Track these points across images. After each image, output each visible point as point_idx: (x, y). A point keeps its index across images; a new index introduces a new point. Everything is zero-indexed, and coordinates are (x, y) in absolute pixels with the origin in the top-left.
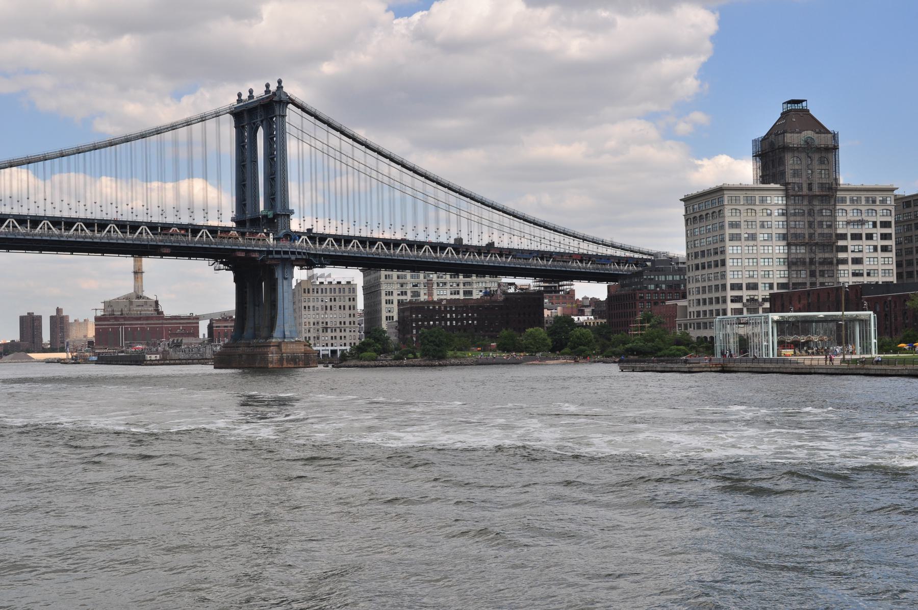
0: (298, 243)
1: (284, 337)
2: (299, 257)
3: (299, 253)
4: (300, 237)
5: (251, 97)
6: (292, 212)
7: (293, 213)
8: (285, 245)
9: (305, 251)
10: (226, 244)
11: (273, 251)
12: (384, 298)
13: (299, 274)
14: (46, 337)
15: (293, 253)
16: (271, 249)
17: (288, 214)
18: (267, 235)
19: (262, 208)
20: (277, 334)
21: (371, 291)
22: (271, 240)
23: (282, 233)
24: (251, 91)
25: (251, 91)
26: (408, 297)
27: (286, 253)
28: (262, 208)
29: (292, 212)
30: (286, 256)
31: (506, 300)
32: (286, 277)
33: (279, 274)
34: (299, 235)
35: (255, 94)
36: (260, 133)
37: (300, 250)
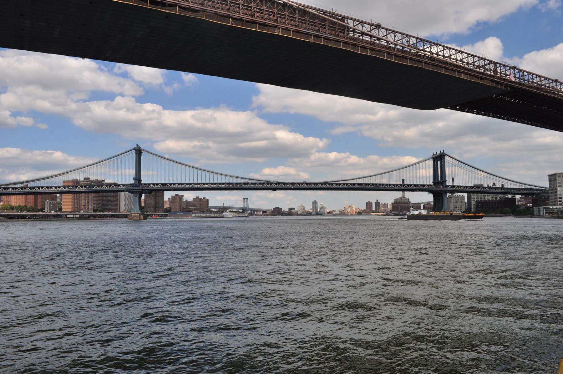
0: (448, 188)
5: (437, 154)
6: (447, 181)
8: (445, 188)
10: (431, 189)
12: (472, 199)
13: (448, 194)
14: (374, 208)
17: (446, 181)
18: (441, 186)
19: (439, 180)
21: (469, 198)
23: (444, 186)
24: (437, 152)
25: (437, 152)
26: (479, 199)
28: (439, 180)
29: (447, 181)
31: (505, 200)
33: (444, 195)
35: (438, 153)
36: (439, 162)
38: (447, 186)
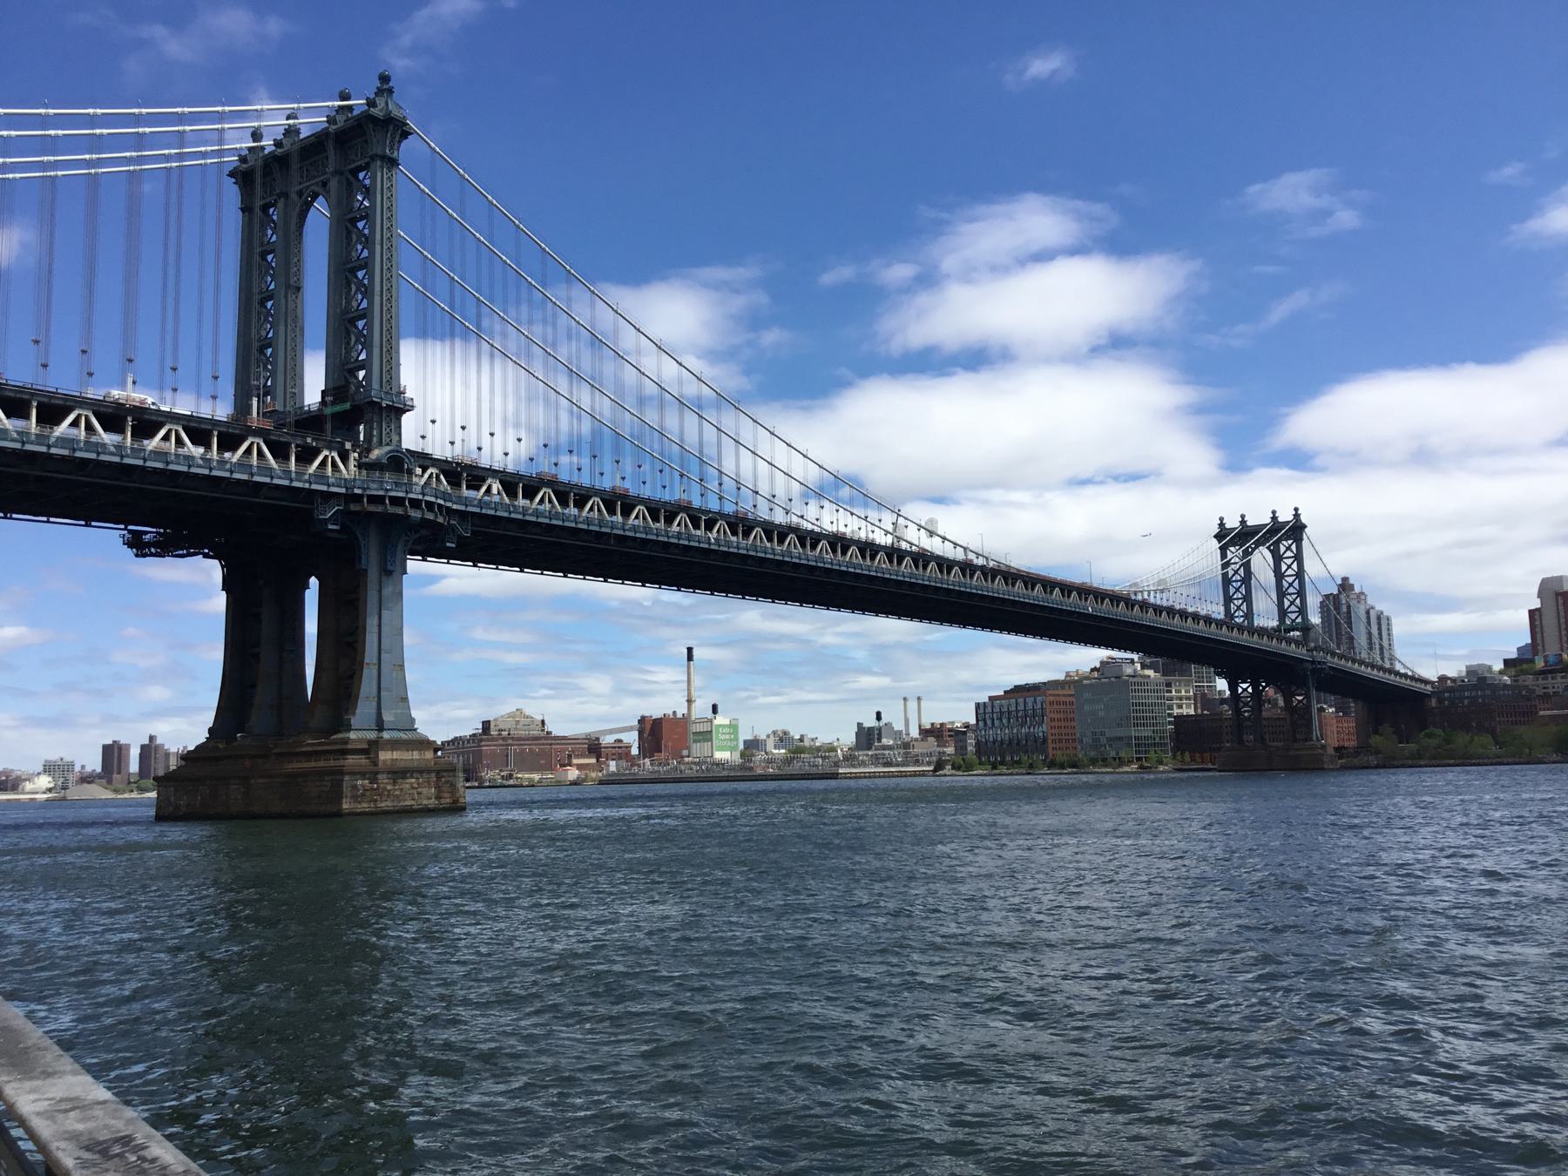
1: (380, 726)
2: (430, 516)
3: (430, 505)
4: (424, 470)
7: (412, 408)
8: (387, 485)
9: (442, 502)
11: (361, 496)
15: (415, 504)
16: (357, 491)
17: (398, 409)
20: (363, 713)
22: (349, 471)
27: (397, 501)
30: (400, 511)
32: (390, 568)
33: (371, 560)
34: (424, 460)
37: (433, 499)
38: (400, 462)
